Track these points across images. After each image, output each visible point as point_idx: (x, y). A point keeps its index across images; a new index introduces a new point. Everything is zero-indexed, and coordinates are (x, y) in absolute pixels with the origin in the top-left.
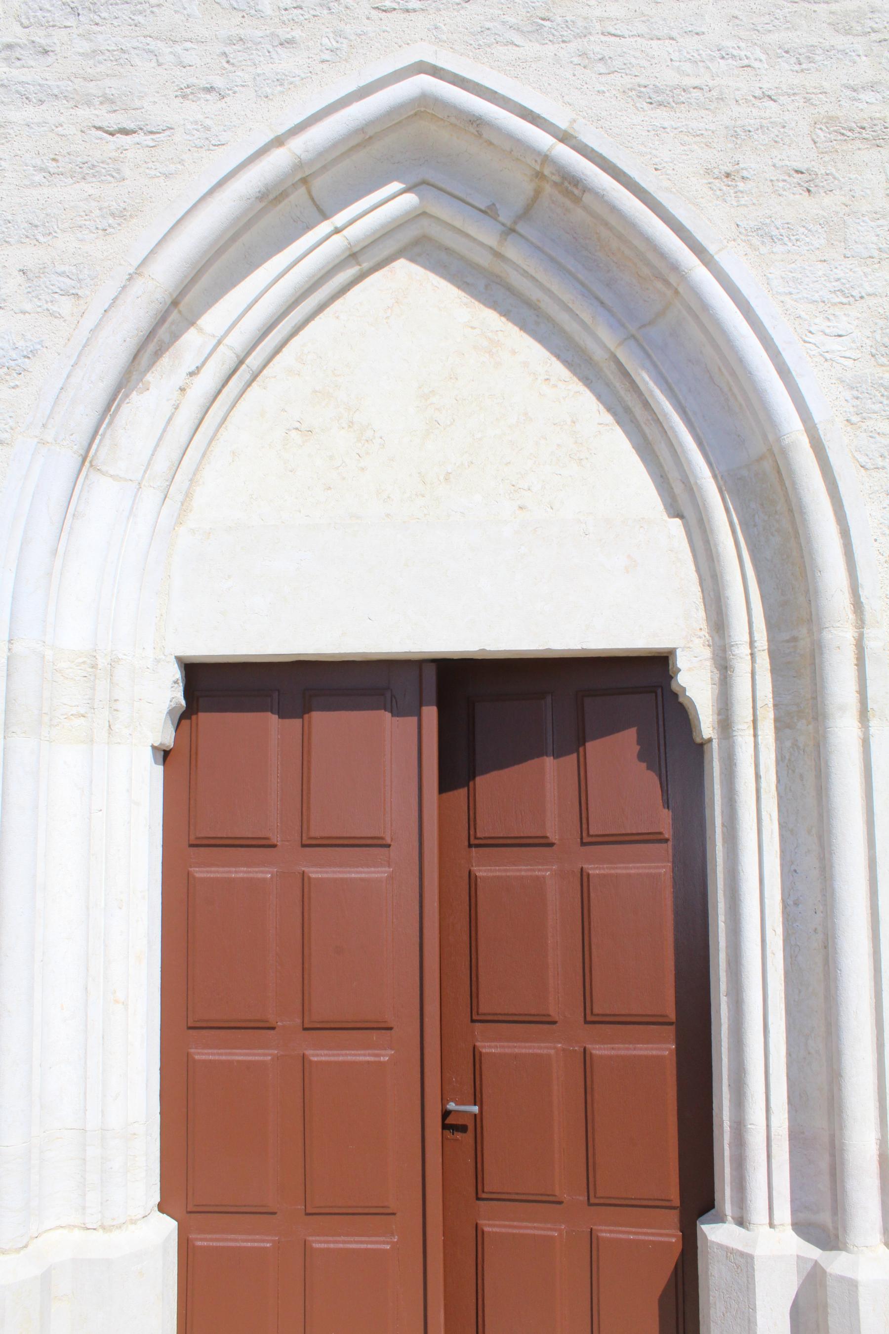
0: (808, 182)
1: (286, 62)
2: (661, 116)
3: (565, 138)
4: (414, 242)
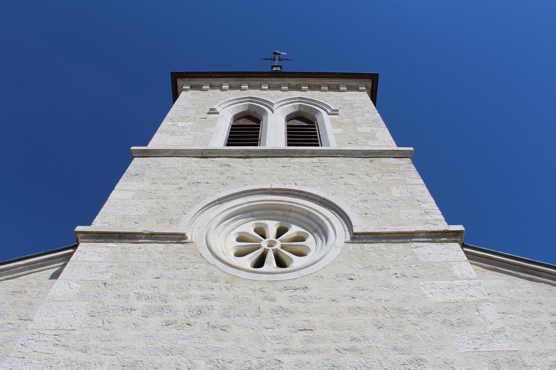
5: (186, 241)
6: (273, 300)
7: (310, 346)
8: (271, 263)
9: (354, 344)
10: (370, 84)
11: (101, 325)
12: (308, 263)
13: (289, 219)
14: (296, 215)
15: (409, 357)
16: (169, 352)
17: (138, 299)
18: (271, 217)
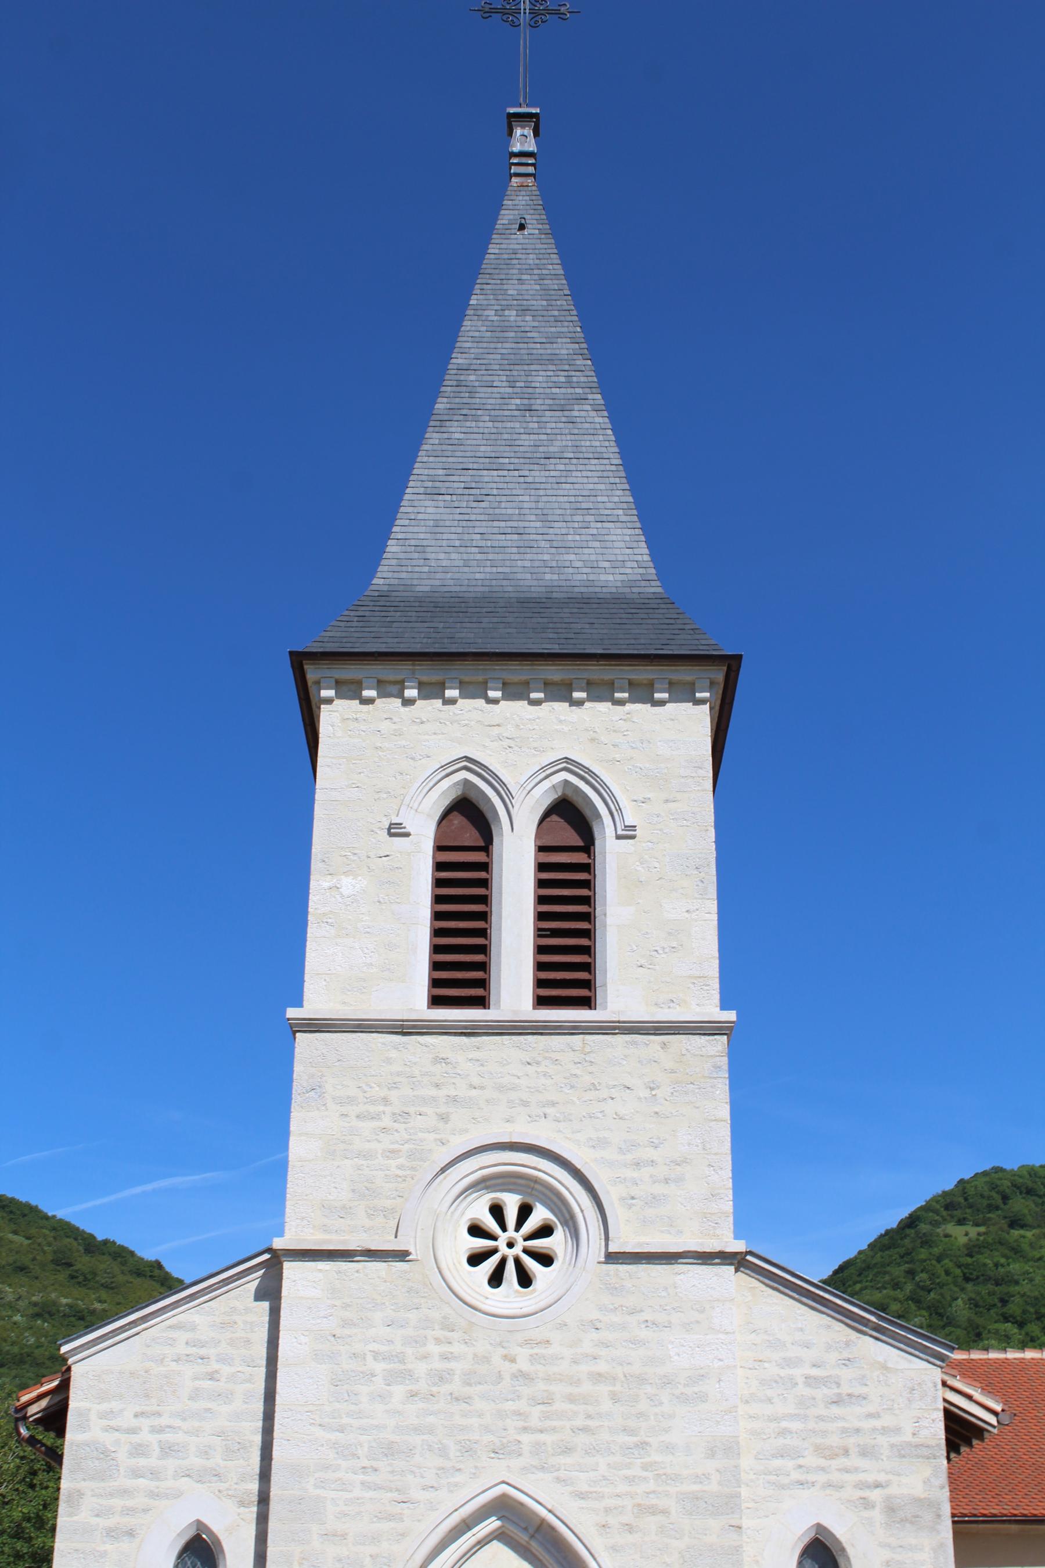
0: (630, 1528)
1: (459, 1478)
2: (583, 1503)
3: (550, 1511)
4: (499, 1536)
6: (513, 1360)
7: (548, 1423)
8: (510, 1283)
9: (589, 1423)
11: (347, 1398)
12: (553, 1301)
13: (534, 1192)
14: (544, 1190)
15: (635, 1439)
16: (417, 1430)
17: (375, 1360)
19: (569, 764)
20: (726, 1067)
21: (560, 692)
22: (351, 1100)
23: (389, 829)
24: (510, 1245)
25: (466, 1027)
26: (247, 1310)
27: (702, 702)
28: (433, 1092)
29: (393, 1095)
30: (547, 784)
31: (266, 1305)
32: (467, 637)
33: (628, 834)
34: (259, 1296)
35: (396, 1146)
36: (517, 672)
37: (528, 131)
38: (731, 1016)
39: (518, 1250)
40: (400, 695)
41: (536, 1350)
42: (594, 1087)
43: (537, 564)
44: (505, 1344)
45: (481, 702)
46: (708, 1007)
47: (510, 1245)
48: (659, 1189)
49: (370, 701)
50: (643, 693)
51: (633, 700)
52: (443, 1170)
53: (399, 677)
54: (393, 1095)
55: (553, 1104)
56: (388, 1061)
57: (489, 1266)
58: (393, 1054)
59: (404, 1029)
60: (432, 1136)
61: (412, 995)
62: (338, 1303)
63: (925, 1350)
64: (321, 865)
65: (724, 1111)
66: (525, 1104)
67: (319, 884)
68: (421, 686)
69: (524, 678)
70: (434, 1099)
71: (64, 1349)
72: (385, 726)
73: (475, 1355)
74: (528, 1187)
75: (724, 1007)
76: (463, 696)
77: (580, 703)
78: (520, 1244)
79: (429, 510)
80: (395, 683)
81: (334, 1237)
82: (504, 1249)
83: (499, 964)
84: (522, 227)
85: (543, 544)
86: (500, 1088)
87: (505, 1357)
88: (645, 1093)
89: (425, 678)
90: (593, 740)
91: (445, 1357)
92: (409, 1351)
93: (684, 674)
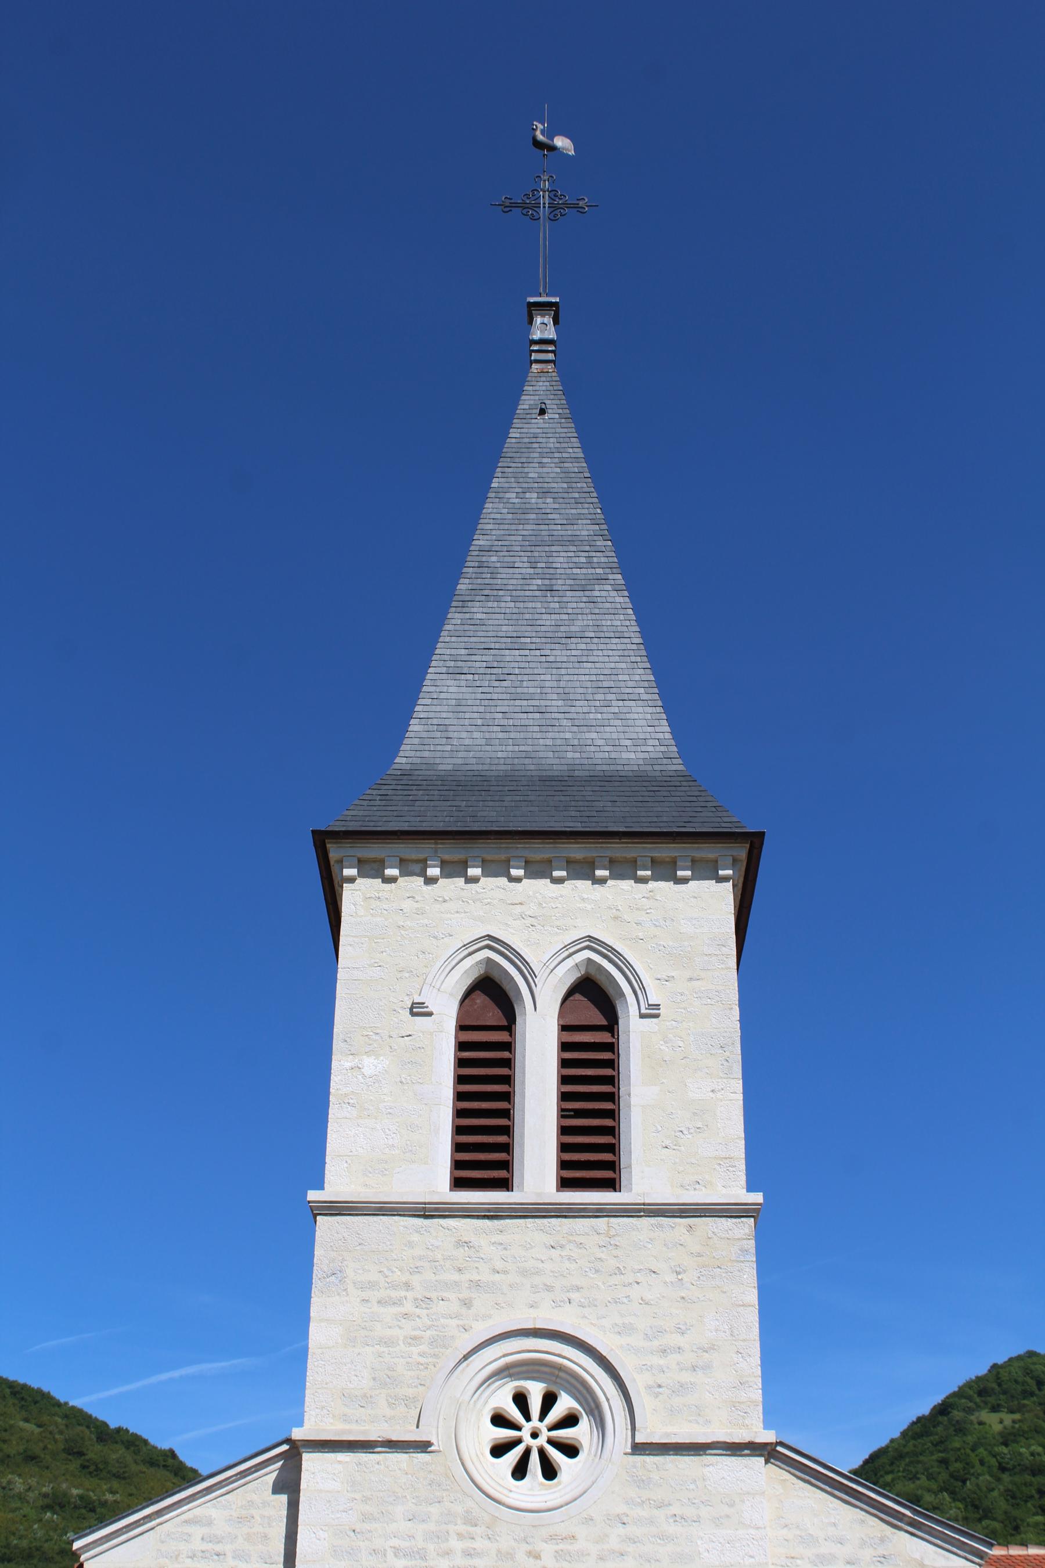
5: (432, 1448)
6: (537, 1557)
8: (535, 1475)
10: (742, 852)
13: (558, 1380)
17: (396, 1556)
18: (535, 1375)
19: (592, 943)
20: (753, 1250)
21: (583, 870)
22: (372, 1285)
23: (411, 1009)
24: (535, 1435)
25: (489, 1210)
26: (266, 1504)
27: (725, 879)
28: (456, 1277)
29: (415, 1280)
30: (570, 963)
31: (284, 1498)
32: (490, 817)
33: (652, 1013)
34: (277, 1489)
35: (417, 1333)
36: (540, 851)
37: (548, 320)
38: (758, 1198)
39: (542, 1441)
40: (423, 873)
41: (561, 1546)
42: (619, 1271)
43: (559, 742)
44: (529, 1540)
45: (503, 881)
46: (734, 1189)
47: (535, 1435)
48: (686, 1377)
49: (393, 880)
50: (666, 871)
51: (655, 878)
52: (466, 1357)
53: (421, 856)
54: (415, 1280)
55: (578, 1289)
56: (411, 1245)
57: (513, 1456)
58: (415, 1238)
59: (426, 1212)
60: (454, 1322)
61: (432, 1175)
62: (358, 1496)
63: (962, 1546)
64: (342, 1045)
65: (752, 1296)
66: (549, 1288)
67: (340, 1064)
68: (443, 864)
69: (547, 856)
70: (456, 1284)
71: (76, 1545)
72: (408, 905)
73: (499, 1551)
74: (552, 1374)
75: (751, 1188)
76: (486, 874)
77: (602, 881)
78: (545, 1435)
79: (451, 689)
80: (418, 861)
81: (354, 1427)
82: (528, 1440)
83: (522, 1145)
84: (542, 412)
85: (565, 722)
86: (524, 1273)
87: (530, 1554)
88: (671, 1278)
89: (446, 857)
90: (616, 918)
91: (468, 1554)
92: (431, 1547)
93: (707, 851)
